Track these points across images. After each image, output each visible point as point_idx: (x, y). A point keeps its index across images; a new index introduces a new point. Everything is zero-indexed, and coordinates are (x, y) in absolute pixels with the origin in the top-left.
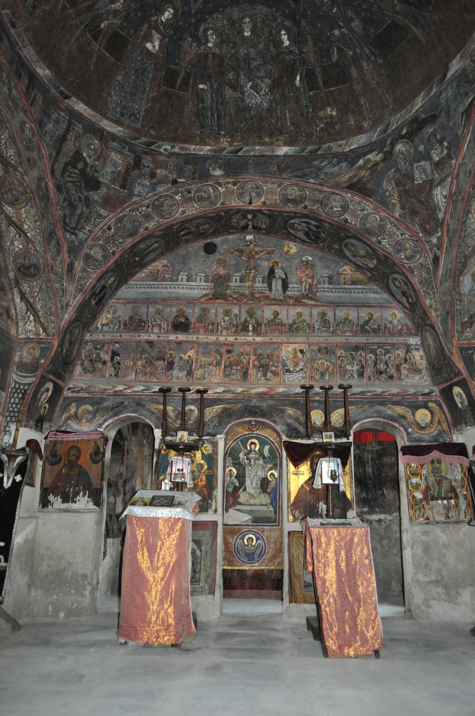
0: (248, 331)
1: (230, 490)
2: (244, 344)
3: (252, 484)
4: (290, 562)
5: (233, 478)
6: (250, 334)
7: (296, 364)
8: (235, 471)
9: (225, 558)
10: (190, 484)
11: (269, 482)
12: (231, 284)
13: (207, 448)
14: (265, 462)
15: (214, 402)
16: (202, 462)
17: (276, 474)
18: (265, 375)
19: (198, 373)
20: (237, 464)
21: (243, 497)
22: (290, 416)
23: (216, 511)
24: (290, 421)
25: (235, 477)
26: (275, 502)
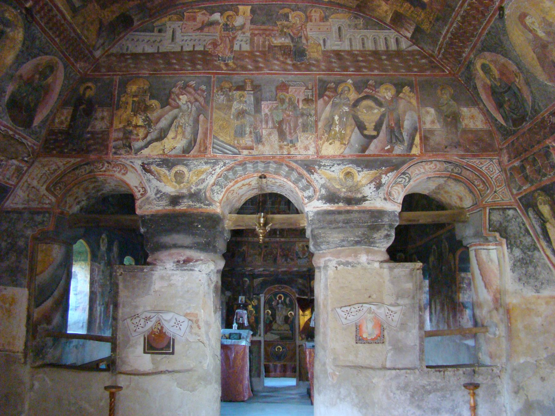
0: (276, 234)
1: (268, 322)
2: (274, 242)
3: (279, 319)
4: (299, 360)
5: (269, 316)
6: (278, 236)
7: (304, 254)
8: (270, 312)
9: (265, 358)
10: (246, 323)
11: (289, 318)
12: (267, 206)
13: (255, 302)
14: (287, 307)
15: (259, 276)
16: (252, 309)
17: (293, 313)
18: (286, 260)
19: (249, 259)
20: (271, 308)
21: (275, 326)
22: (300, 284)
23: (260, 335)
24: (300, 286)
25: (271, 315)
26: (292, 329)
